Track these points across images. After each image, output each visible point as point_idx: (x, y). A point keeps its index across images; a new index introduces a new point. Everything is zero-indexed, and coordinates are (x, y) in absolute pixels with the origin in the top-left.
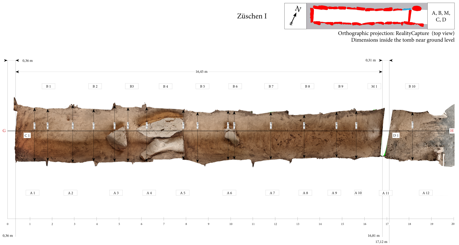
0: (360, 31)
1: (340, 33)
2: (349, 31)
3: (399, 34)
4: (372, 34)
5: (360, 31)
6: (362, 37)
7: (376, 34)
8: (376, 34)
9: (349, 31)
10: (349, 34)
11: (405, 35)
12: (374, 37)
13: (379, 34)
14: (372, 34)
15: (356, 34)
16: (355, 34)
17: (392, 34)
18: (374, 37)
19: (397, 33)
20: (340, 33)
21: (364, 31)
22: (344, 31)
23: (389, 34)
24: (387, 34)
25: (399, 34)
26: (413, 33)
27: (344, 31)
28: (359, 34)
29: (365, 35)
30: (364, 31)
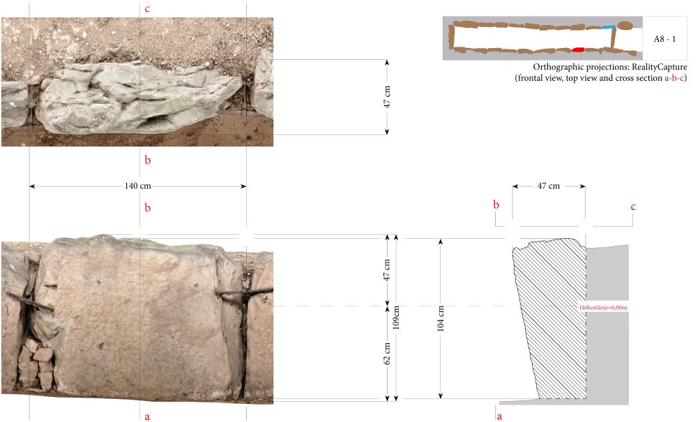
1: (537, 67)
2: (552, 63)
3: (637, 67)
6: (573, 73)
7: (596, 68)
8: (596, 68)
9: (552, 63)
10: (551, 68)
12: (592, 73)
13: (601, 68)
15: (563, 68)
17: (626, 68)
18: (592, 73)
19: (634, 67)
20: (537, 67)
22: (542, 63)
23: (617, 68)
24: (614, 68)
25: (637, 67)
27: (542, 63)
28: (568, 68)
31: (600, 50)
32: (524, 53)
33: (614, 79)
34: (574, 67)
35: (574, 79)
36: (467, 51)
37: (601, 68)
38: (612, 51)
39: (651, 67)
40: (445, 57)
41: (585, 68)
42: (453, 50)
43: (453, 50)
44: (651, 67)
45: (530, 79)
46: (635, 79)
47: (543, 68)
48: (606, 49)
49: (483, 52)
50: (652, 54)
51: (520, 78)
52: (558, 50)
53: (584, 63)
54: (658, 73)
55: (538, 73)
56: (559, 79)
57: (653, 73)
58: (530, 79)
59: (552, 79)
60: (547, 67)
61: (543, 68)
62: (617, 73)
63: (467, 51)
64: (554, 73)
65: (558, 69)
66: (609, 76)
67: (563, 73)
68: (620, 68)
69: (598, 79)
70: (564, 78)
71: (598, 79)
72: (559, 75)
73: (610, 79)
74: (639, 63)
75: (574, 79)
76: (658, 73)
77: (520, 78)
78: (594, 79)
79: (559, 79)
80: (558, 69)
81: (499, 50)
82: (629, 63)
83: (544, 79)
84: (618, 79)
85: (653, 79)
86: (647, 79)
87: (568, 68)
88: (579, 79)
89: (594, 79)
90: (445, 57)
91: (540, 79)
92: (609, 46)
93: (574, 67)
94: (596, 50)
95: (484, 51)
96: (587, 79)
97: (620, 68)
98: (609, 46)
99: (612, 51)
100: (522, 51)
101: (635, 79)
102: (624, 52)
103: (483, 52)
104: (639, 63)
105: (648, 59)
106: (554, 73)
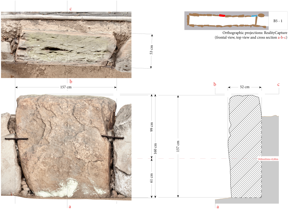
0: (238, 31)
1: (224, 33)
2: (230, 31)
3: (266, 33)
4: (246, 33)
5: (238, 31)
6: (239, 35)
9: (230, 31)
10: (230, 33)
11: (271, 34)
12: (247, 35)
13: (251, 33)
14: (246, 33)
15: (235, 33)
16: (234, 33)
18: (247, 35)
19: (265, 33)
20: (224, 33)
21: (241, 31)
22: (226, 31)
24: (257, 33)
26: (276, 33)
27: (226, 31)
28: (237, 33)
29: (241, 34)
30: (241, 31)
31: (251, 26)
32: (219, 27)
33: (257, 38)
34: (240, 33)
35: (240, 38)
36: (195, 26)
37: (251, 33)
38: (256, 26)
39: (272, 33)
40: (185, 29)
41: (244, 33)
42: (189, 26)
43: (189, 26)
44: (272, 33)
45: (221, 38)
46: (265, 38)
47: (227, 33)
48: (253, 25)
49: (202, 27)
50: (273, 27)
51: (217, 37)
52: (233, 25)
53: (244, 31)
54: (275, 35)
55: (224, 35)
56: (233, 38)
57: (273, 35)
58: (221, 38)
59: (231, 38)
60: (228, 33)
61: (227, 33)
62: (258, 35)
63: (195, 26)
64: (231, 35)
65: (233, 33)
66: (254, 37)
67: (235, 35)
68: (259, 33)
69: (250, 38)
70: (236, 38)
71: (250, 38)
72: (233, 36)
73: (255, 38)
74: (267, 31)
75: (240, 38)
76: (275, 35)
77: (217, 37)
78: (248, 38)
79: (233, 38)
80: (233, 33)
81: (208, 26)
82: (263, 31)
83: (227, 38)
84: (258, 38)
85: (273, 38)
86: (270, 38)
87: (237, 33)
88: (242, 38)
89: (248, 38)
90: (185, 29)
91: (225, 38)
92: (255, 24)
93: (240, 33)
94: (249, 26)
95: (202, 26)
96: (245, 38)
97: (259, 33)
98: (255, 24)
99: (256, 26)
100: (218, 26)
101: (265, 38)
102: (261, 26)
103: (202, 27)
104: (267, 31)
105: (271, 29)
106: (231, 35)
